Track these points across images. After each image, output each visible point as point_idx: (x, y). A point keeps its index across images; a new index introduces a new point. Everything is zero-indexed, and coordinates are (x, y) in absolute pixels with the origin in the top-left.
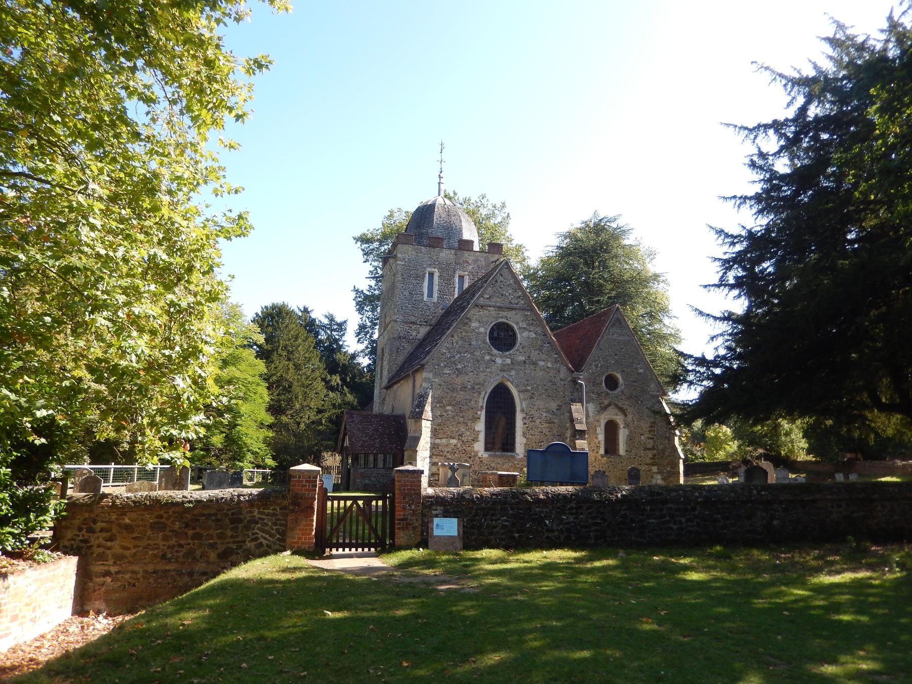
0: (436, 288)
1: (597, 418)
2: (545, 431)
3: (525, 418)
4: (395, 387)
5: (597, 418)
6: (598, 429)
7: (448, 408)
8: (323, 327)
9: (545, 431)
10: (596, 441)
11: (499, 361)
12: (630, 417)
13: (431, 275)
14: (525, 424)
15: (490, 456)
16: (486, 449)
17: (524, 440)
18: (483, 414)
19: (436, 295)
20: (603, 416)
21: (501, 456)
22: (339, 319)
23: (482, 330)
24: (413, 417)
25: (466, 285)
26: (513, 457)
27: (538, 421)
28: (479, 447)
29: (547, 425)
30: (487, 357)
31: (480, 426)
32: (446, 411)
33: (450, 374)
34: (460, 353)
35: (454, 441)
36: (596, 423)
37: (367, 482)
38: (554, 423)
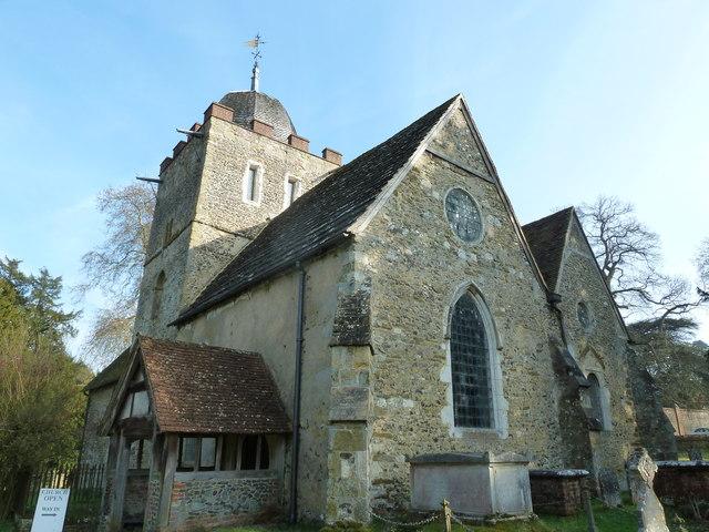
0: (260, 189)
4: (212, 315)
7: (397, 331)
8: (32, 281)
11: (462, 254)
13: (254, 170)
15: (464, 433)
16: (459, 422)
18: (446, 347)
19: (260, 195)
22: (53, 275)
23: (436, 195)
24: (344, 343)
25: (298, 194)
26: (496, 436)
27: (519, 369)
28: (447, 414)
30: (447, 245)
31: (446, 374)
32: (393, 338)
33: (396, 263)
34: (409, 227)
35: (409, 404)
37: (196, 506)
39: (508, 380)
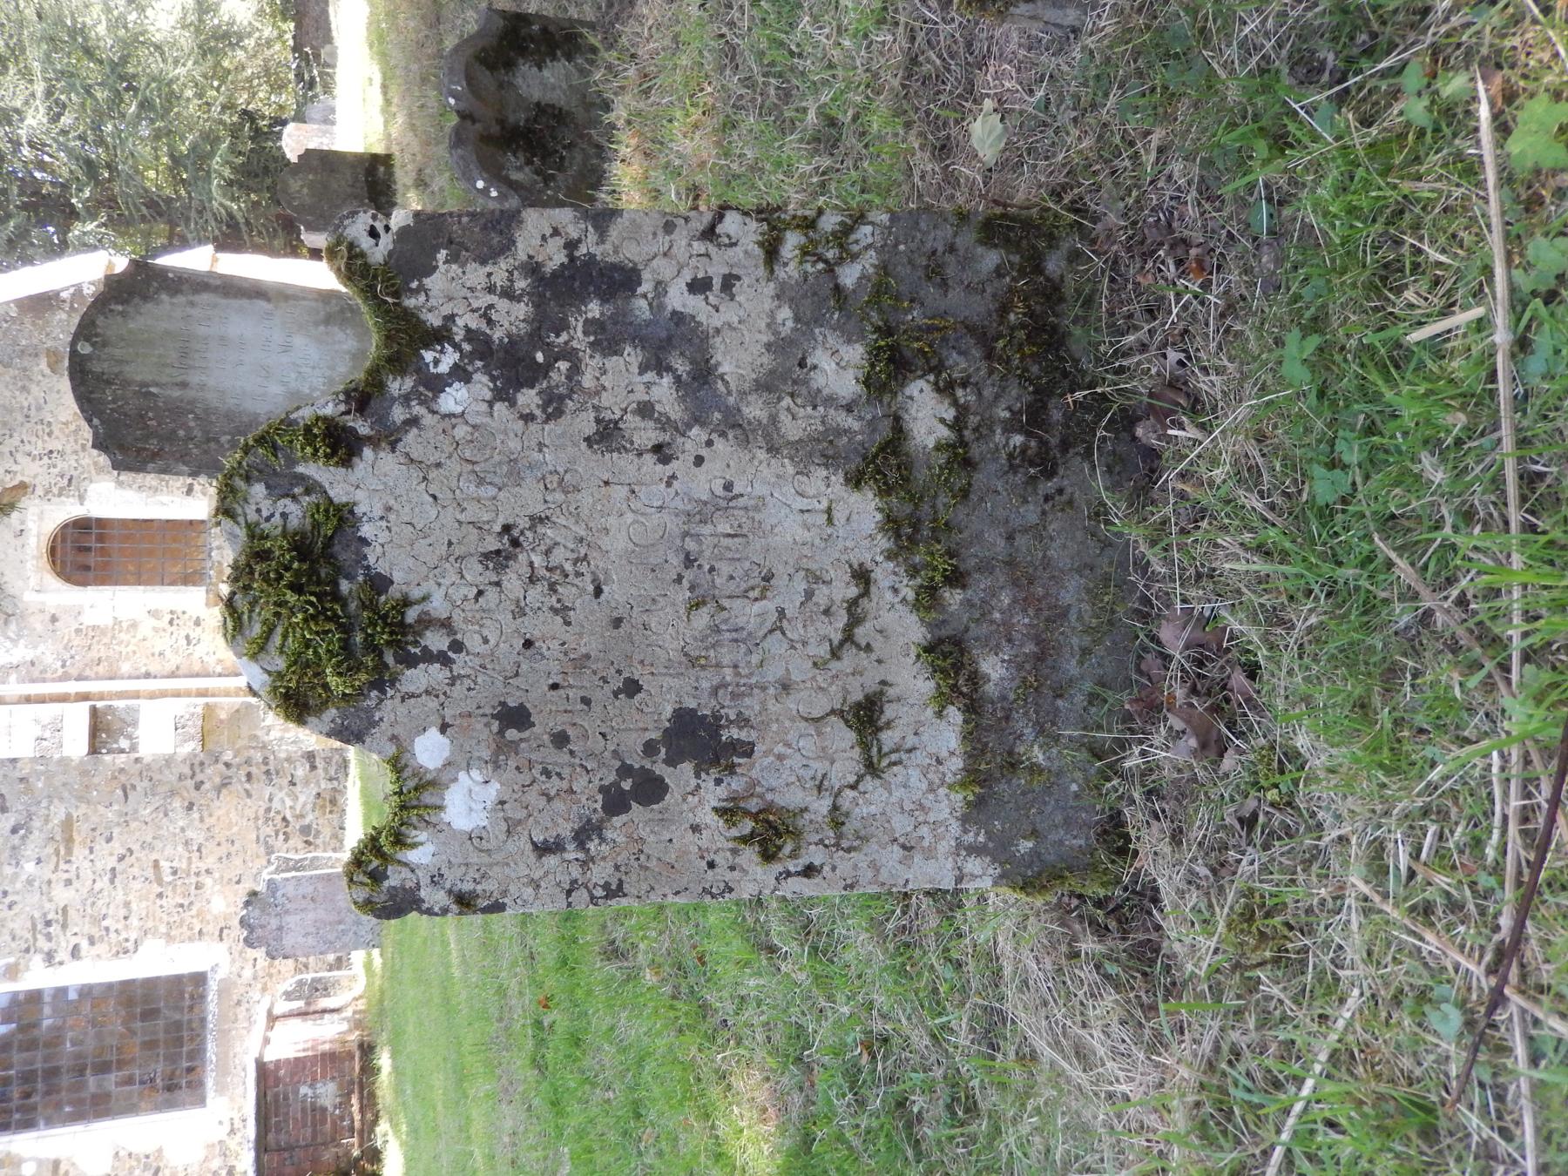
1: (37, 623)
2: (106, 857)
3: (49, 957)
5: (37, 623)
6: (88, 619)
9: (106, 857)
10: (146, 628)
12: (28, 470)
14: (75, 953)
15: (221, 1089)
17: (151, 946)
20: (29, 597)
21: (224, 1034)
27: (62, 895)
29: (79, 852)
36: (66, 627)
38: (68, 824)
39: (92, 942)
